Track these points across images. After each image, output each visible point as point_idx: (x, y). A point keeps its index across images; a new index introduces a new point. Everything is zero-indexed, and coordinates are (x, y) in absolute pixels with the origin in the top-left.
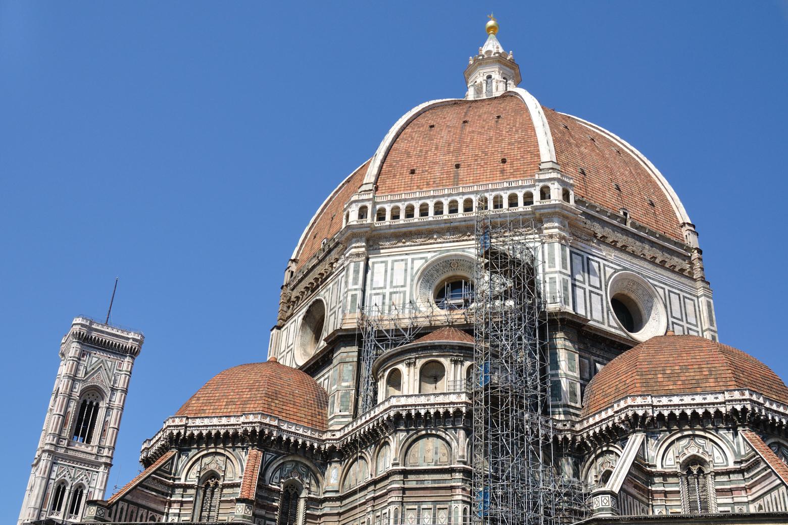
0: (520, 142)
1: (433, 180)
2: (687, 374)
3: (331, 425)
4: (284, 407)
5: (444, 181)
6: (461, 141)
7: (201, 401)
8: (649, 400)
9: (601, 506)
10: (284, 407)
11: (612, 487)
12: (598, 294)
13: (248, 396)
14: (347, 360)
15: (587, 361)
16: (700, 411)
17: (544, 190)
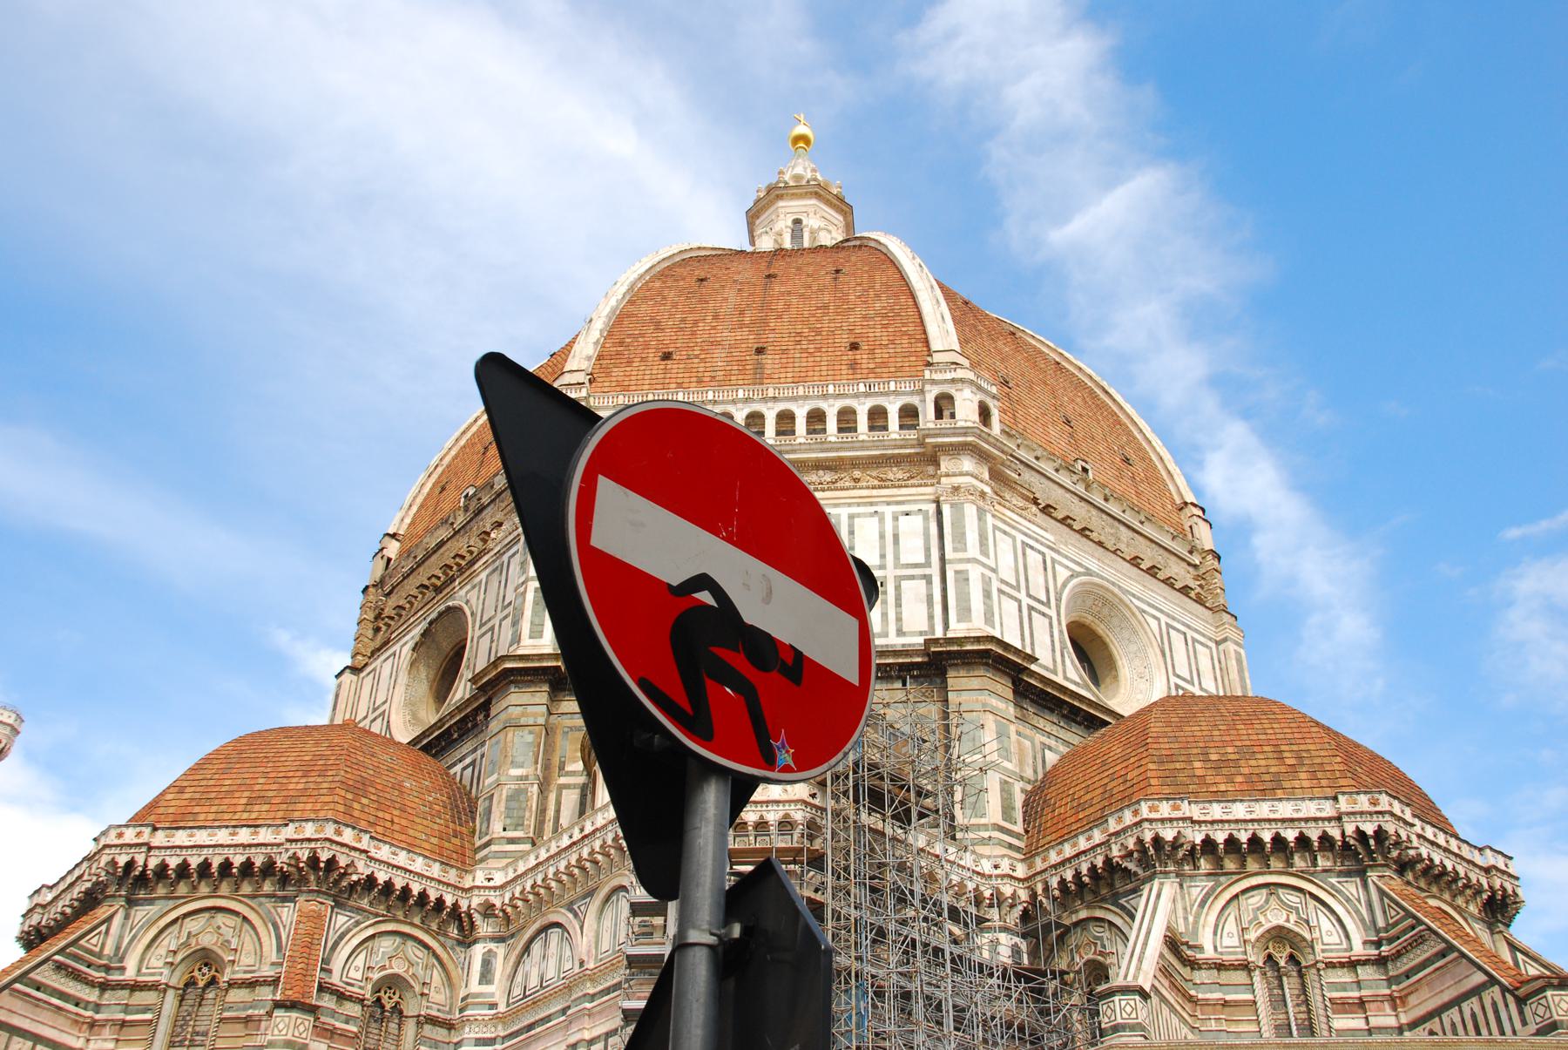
0: (885, 316)
1: (709, 374)
2: (1253, 763)
3: (482, 860)
4: (380, 814)
5: (733, 378)
6: (765, 307)
7: (187, 796)
8: (1188, 809)
9: (1119, 1020)
10: (380, 814)
11: (1135, 977)
12: (1044, 614)
13: (300, 786)
14: (523, 721)
15: (1027, 743)
16: (1290, 835)
17: (943, 403)
